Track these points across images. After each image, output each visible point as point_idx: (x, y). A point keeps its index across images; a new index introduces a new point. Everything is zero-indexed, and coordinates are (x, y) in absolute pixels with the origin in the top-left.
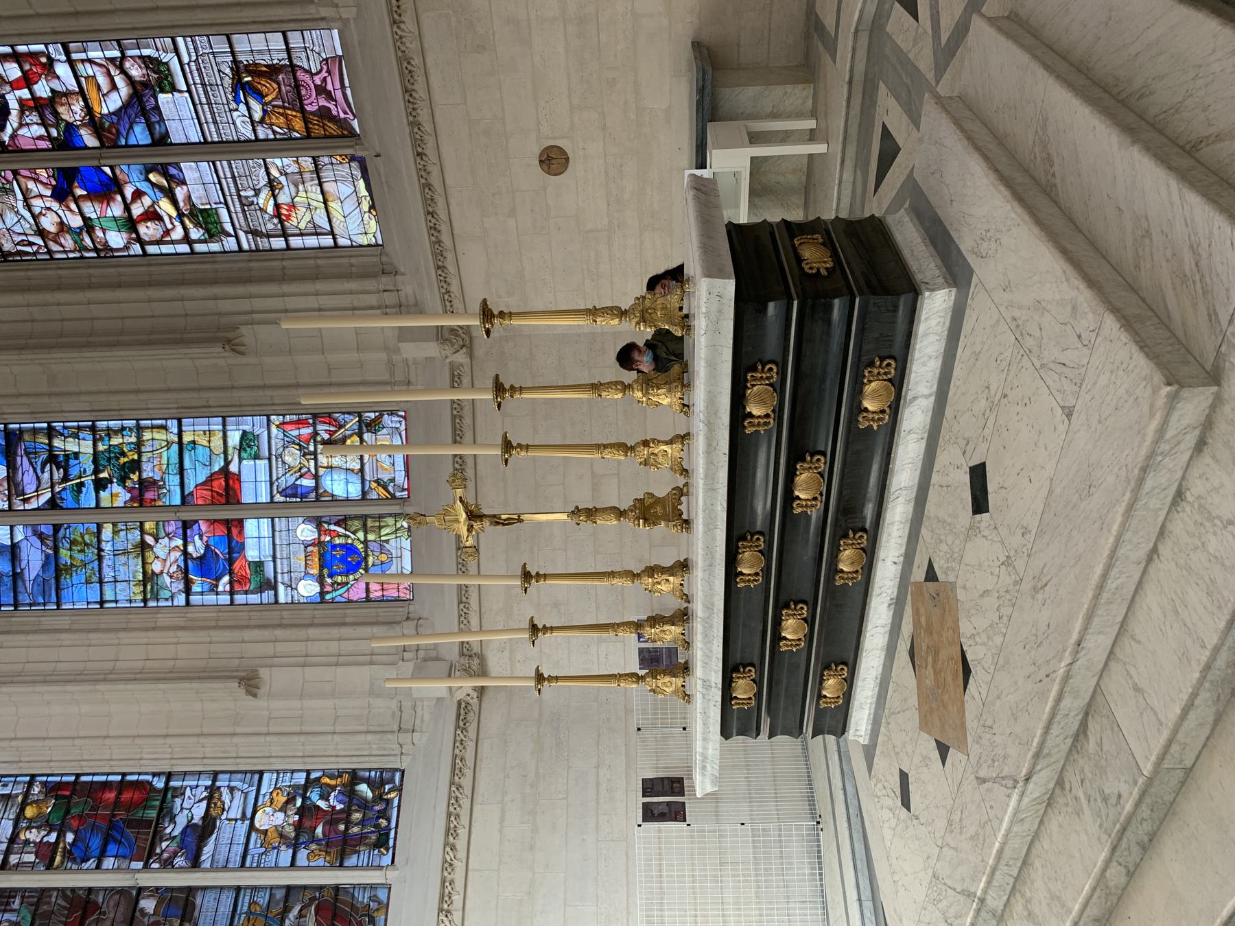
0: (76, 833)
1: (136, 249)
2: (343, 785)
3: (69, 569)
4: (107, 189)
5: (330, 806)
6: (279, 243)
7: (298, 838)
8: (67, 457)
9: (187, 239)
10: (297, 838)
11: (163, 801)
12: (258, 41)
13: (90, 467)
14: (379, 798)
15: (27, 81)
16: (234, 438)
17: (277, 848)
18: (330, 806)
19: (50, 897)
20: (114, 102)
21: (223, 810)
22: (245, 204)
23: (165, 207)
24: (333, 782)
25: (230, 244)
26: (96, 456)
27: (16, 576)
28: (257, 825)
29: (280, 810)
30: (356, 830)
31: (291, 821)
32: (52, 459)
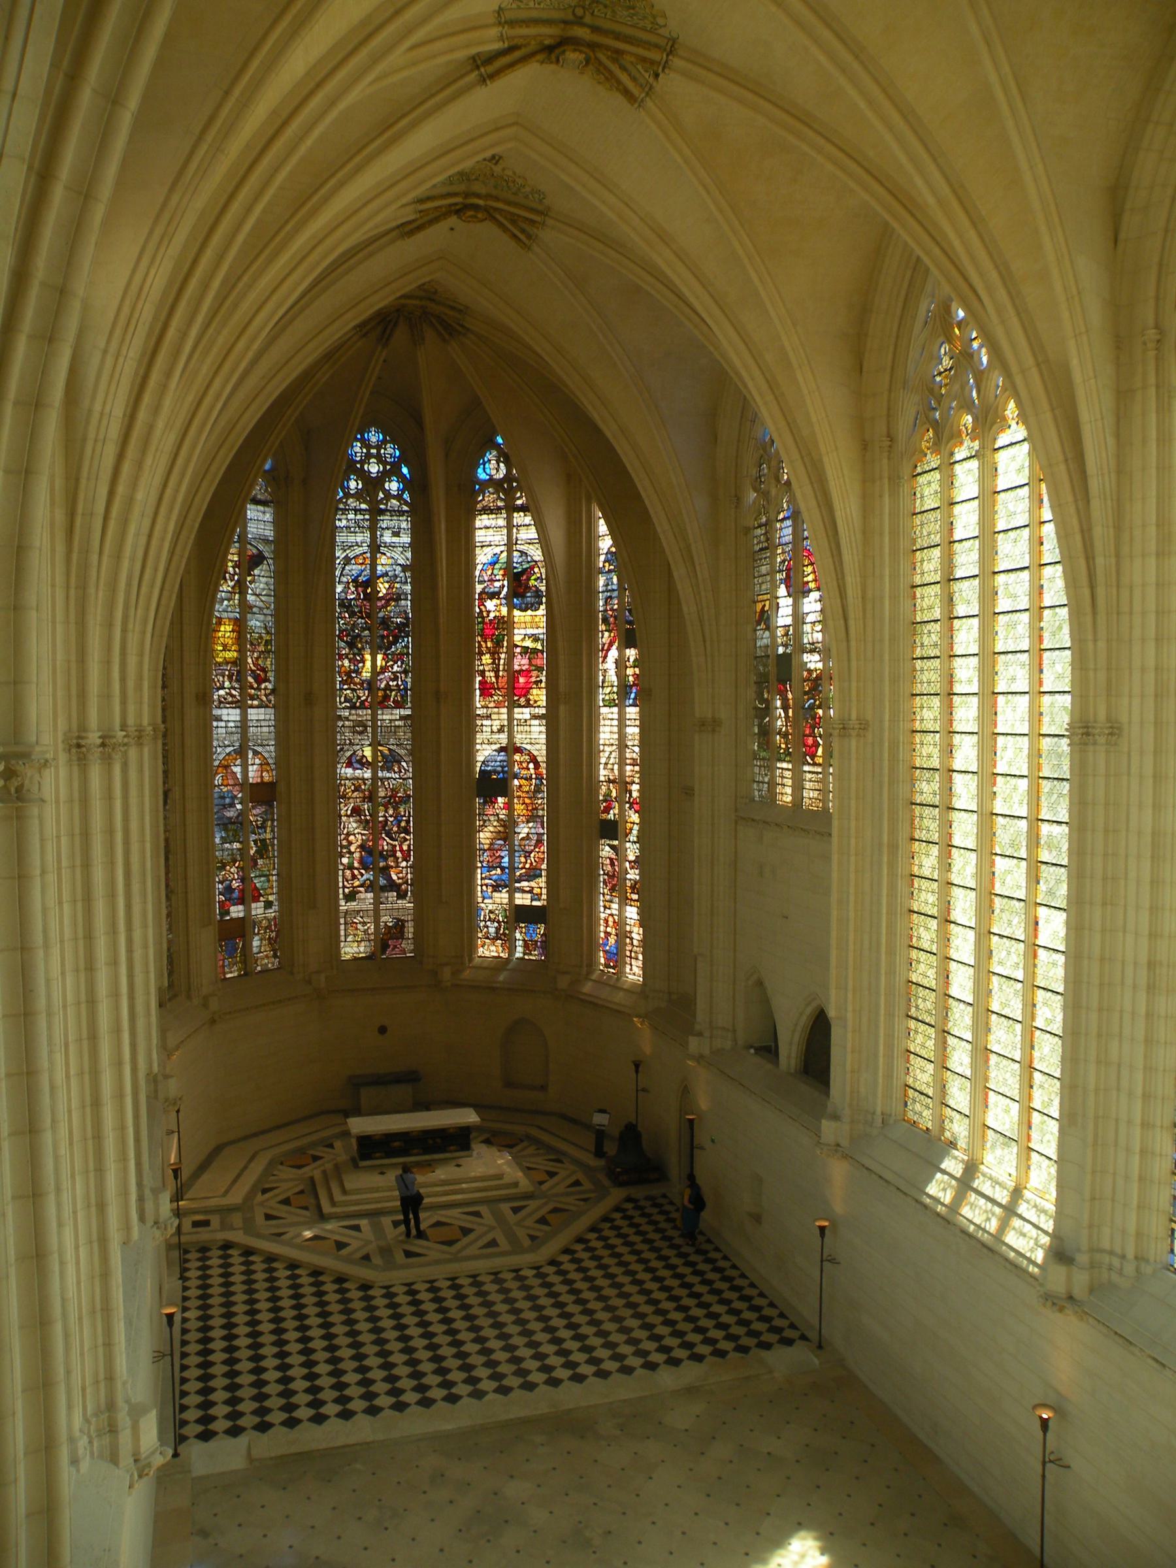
1: (341, 867)
3: (226, 830)
4: (364, 865)
6: (342, 921)
8: (265, 828)
9: (344, 887)
12: (411, 930)
13: (262, 837)
15: (401, 850)
16: (271, 898)
20: (394, 877)
22: (358, 912)
23: (357, 883)
25: (342, 903)
26: (265, 840)
27: (224, 806)
32: (264, 821)
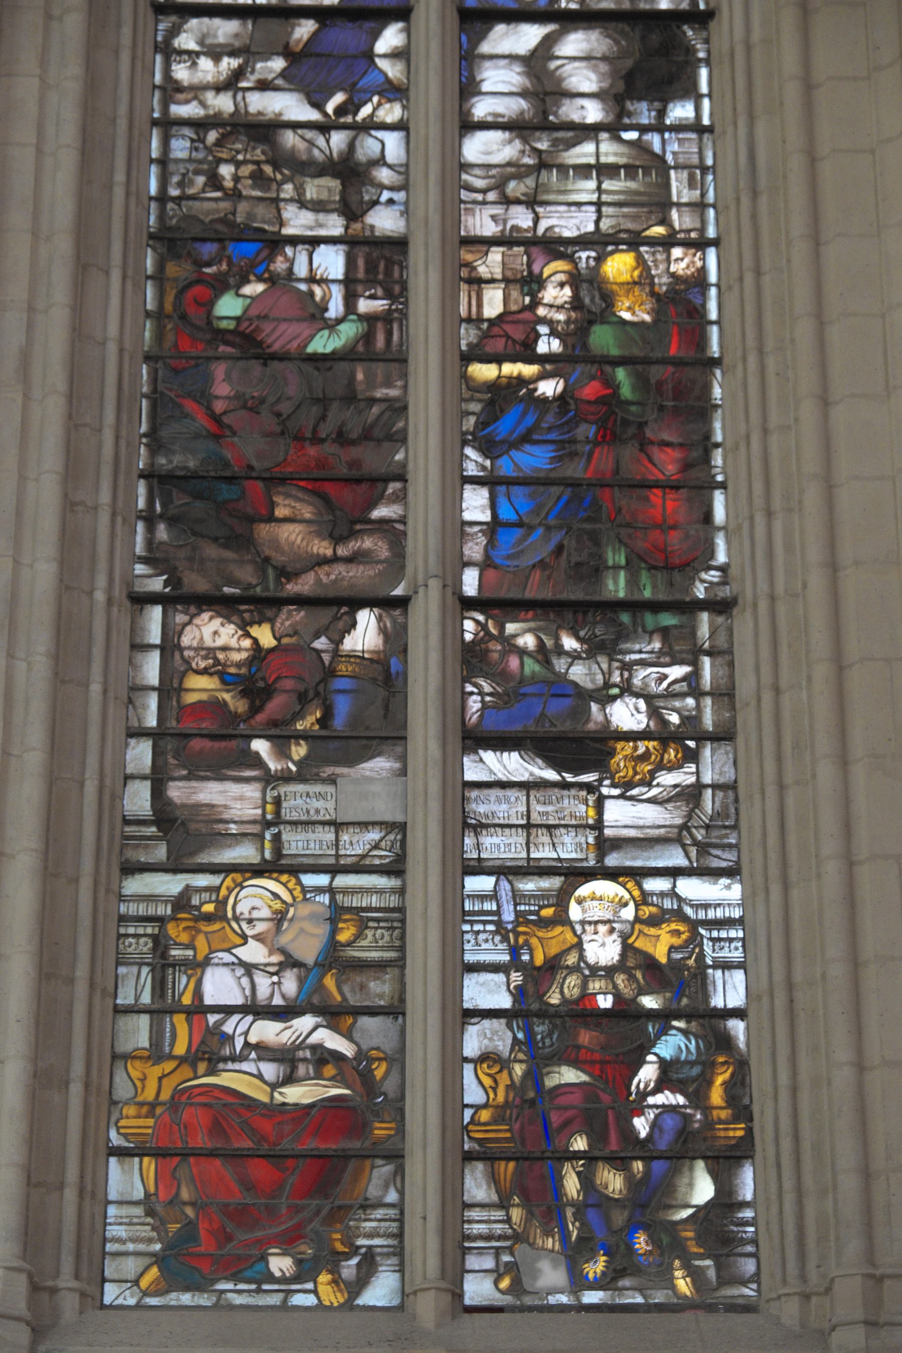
0: (561, 399)
2: (709, 1124)
5: (643, 1095)
7: (544, 1016)
10: (546, 1013)
11: (656, 607)
14: (669, 1242)
17: (515, 963)
18: (643, 1095)
19: (389, 384)
21: (629, 785)
24: (716, 1096)
28: (584, 890)
29: (627, 948)
30: (572, 1185)
31: (595, 985)
